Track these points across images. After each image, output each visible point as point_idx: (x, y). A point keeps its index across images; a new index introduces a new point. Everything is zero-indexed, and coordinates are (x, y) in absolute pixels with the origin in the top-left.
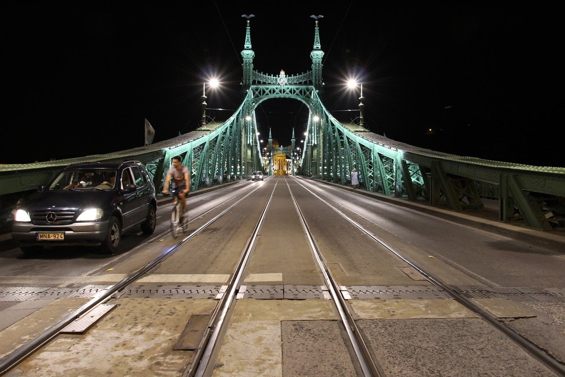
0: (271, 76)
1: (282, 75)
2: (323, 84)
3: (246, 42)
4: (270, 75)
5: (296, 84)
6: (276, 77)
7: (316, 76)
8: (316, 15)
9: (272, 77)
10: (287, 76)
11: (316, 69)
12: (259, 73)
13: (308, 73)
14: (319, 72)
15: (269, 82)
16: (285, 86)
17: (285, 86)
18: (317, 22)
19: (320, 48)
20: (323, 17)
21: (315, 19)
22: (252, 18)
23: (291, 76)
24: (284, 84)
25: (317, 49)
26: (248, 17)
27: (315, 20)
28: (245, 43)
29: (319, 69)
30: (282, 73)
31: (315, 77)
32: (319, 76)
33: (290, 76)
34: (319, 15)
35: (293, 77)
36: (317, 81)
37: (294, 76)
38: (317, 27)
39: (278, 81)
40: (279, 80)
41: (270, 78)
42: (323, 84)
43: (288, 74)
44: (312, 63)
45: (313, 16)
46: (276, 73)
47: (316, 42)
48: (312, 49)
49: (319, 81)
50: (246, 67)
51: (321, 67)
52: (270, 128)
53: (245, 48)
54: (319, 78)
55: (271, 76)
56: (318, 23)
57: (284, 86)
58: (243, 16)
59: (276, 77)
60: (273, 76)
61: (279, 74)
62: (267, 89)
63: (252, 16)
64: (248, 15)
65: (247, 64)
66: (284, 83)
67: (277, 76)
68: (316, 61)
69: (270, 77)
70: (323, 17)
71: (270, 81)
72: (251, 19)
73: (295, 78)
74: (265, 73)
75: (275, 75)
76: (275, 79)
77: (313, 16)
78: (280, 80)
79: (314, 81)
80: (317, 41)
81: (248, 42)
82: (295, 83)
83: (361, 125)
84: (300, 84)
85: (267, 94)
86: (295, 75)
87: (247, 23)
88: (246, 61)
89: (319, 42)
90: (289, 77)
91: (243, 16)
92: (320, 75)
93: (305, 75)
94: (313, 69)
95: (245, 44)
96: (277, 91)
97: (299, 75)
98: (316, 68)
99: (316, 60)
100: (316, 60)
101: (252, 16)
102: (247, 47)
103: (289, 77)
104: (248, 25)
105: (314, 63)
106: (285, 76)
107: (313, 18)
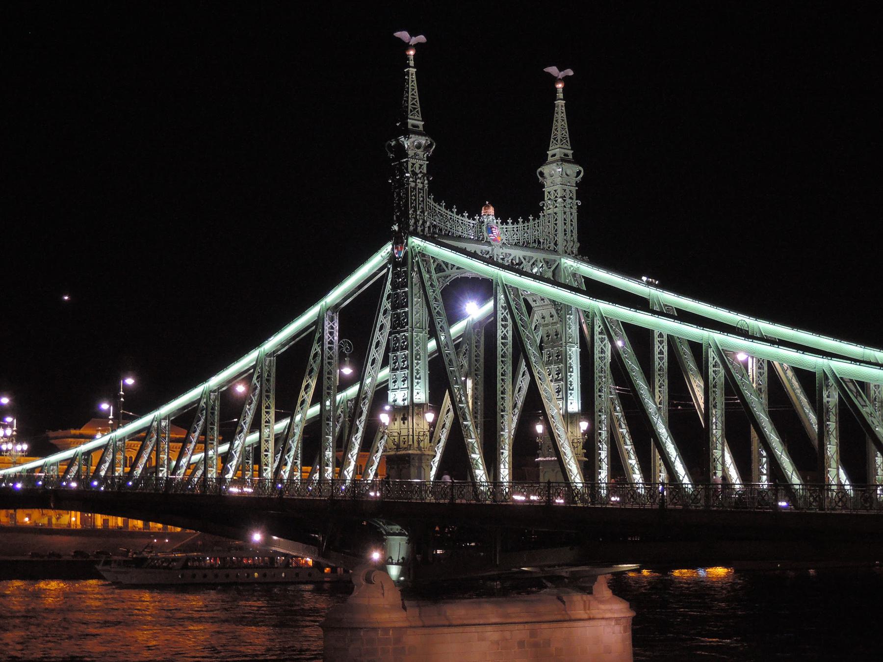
0: (463, 216)
3: (411, 111)
4: (460, 212)
7: (565, 231)
8: (561, 70)
10: (499, 221)
18: (560, 86)
25: (564, 160)
27: (554, 80)
29: (571, 214)
38: (561, 99)
39: (485, 234)
41: (460, 221)
45: (553, 70)
46: (474, 211)
50: (413, 181)
53: (410, 127)
58: (398, 34)
60: (469, 217)
63: (422, 38)
64: (413, 34)
69: (459, 217)
74: (449, 207)
77: (553, 70)
87: (407, 58)
88: (413, 164)
90: (502, 223)
91: (398, 34)
95: (410, 116)
98: (567, 210)
101: (422, 38)
102: (414, 126)
104: (412, 63)
107: (549, 74)
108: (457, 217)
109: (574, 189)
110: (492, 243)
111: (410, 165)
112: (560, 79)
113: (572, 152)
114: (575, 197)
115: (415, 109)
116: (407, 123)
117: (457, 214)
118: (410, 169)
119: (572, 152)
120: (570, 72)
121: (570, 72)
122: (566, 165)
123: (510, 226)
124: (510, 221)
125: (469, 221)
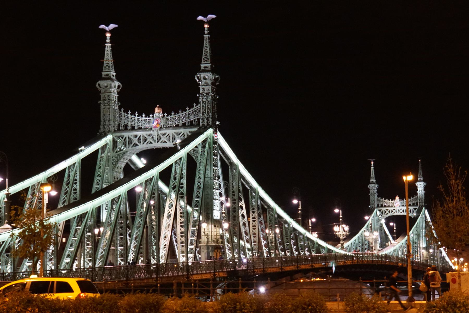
0: (142, 116)
2: (218, 123)
3: (105, 67)
5: (177, 126)
6: (149, 117)
8: (205, 16)
9: (144, 118)
10: (166, 115)
11: (203, 102)
12: (125, 113)
13: (195, 108)
14: (208, 106)
15: (140, 126)
16: (158, 131)
17: (158, 131)
18: (206, 26)
19: (210, 68)
20: (214, 16)
21: (204, 21)
22: (114, 29)
23: (171, 115)
24: (158, 128)
26: (107, 29)
27: (202, 22)
28: (102, 69)
30: (157, 110)
31: (203, 114)
32: (208, 112)
33: (169, 114)
34: (208, 15)
35: (173, 116)
36: (205, 120)
37: (175, 114)
38: (206, 34)
39: (151, 124)
40: (152, 122)
42: (218, 123)
43: (167, 111)
44: (199, 93)
45: (200, 18)
46: (149, 112)
47: (204, 59)
48: (199, 70)
51: (210, 97)
52: (371, 162)
55: (142, 116)
56: (209, 29)
57: (157, 131)
59: (149, 117)
61: (153, 113)
62: (136, 136)
63: (112, 26)
64: (107, 25)
65: (105, 102)
66: (159, 126)
67: (151, 116)
68: (203, 89)
70: (214, 16)
71: (140, 124)
72: (111, 31)
73: (177, 118)
74: (133, 113)
75: (147, 115)
76: (148, 120)
77: (200, 18)
78: (153, 123)
79: (201, 121)
80: (206, 57)
81: (107, 67)
82: (177, 124)
83: (6, 222)
84: (184, 126)
85: (137, 145)
86: (177, 112)
87: (105, 37)
89: (208, 59)
92: (210, 110)
93: (191, 112)
94: (200, 100)
95: (104, 71)
96: (149, 139)
97: (182, 112)
98: (204, 100)
99: (203, 87)
100: (203, 87)
101: (112, 26)
103: (168, 116)
105: (201, 92)
106: (161, 115)
108: (138, 118)
109: (210, 88)
110: (153, 129)
112: (206, 22)
113: (210, 64)
114: (210, 91)
115: (107, 66)
116: (102, 74)
117: (138, 116)
118: (102, 99)
119: (210, 64)
120: (211, 16)
121: (211, 16)
122: (202, 75)
124: (173, 113)
125: (146, 118)
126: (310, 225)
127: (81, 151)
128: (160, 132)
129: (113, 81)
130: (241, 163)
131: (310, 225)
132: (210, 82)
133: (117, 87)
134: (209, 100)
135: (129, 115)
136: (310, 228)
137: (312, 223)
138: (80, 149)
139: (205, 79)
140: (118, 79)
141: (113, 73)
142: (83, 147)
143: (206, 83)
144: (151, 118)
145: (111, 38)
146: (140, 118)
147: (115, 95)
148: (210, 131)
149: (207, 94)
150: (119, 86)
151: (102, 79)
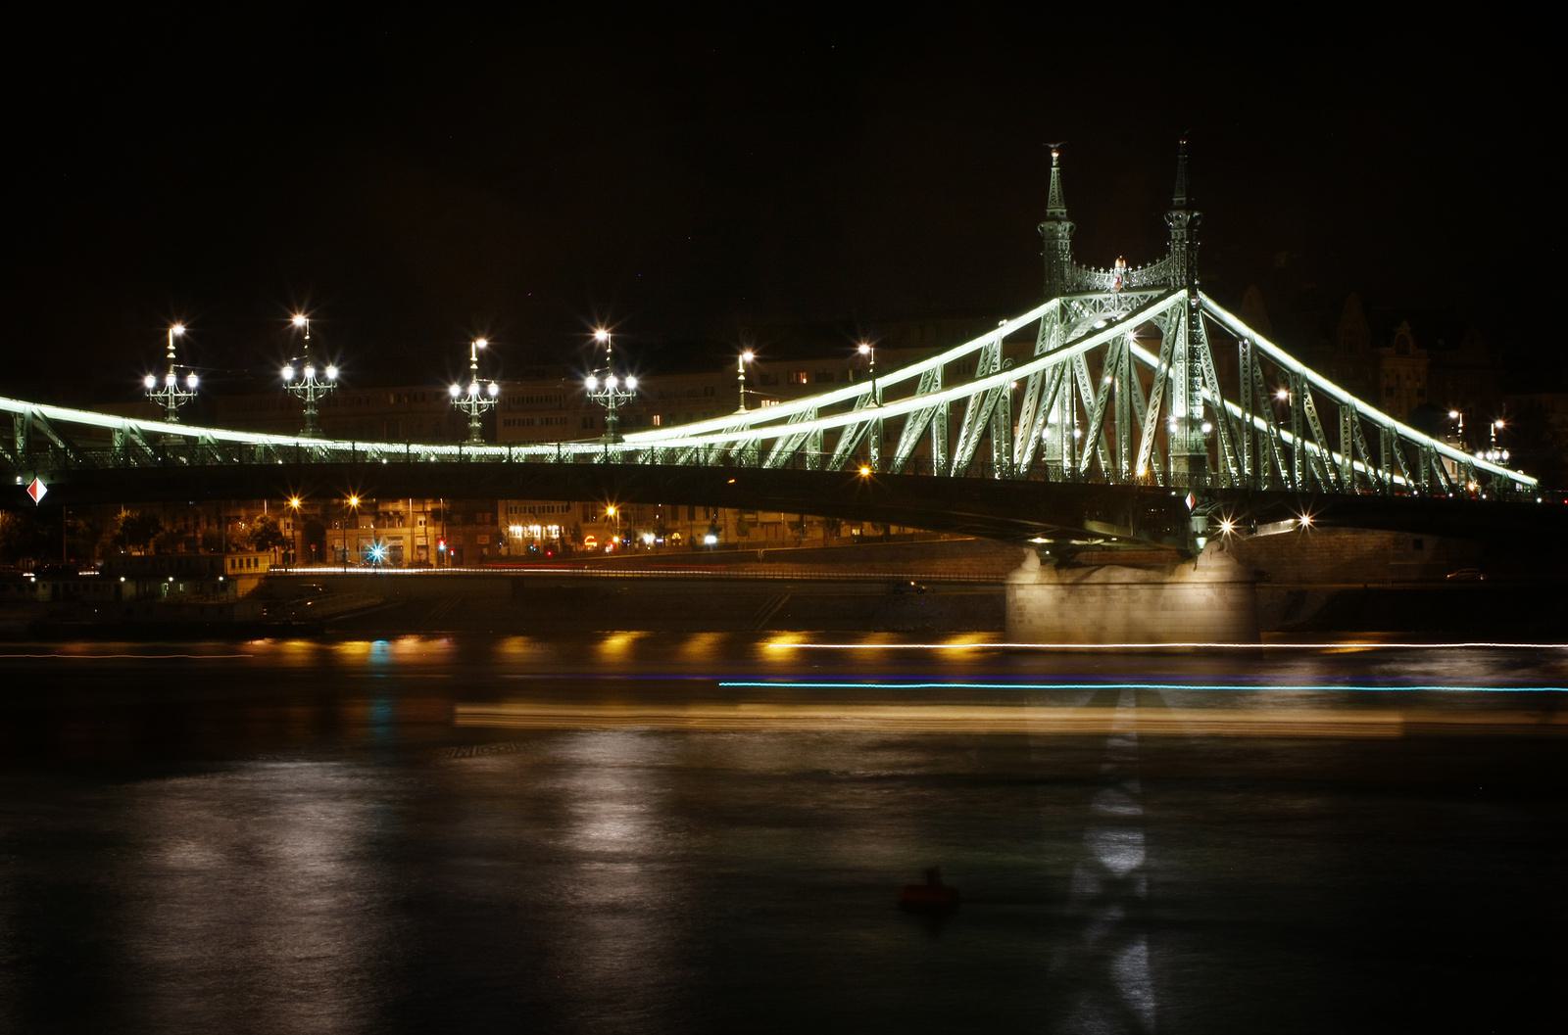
1: (1118, 270)
4: (1097, 270)
6: (1109, 272)
29: (1182, 252)
30: (1118, 263)
43: (1132, 263)
44: (1169, 239)
46: (1109, 266)
49: (1180, 277)
53: (1048, 215)
54: (1182, 270)
59: (1109, 272)
61: (1114, 267)
67: (1111, 271)
75: (1107, 270)
105: (1173, 237)
109: (1184, 231)
111: (1046, 245)
123: (1102, 274)
126: (1493, 434)
127: (1002, 325)
128: (1122, 295)
129: (1059, 221)
130: (1268, 339)
131: (1493, 434)
132: (1184, 224)
133: (1068, 230)
134: (1183, 249)
135: (1084, 271)
136: (1493, 440)
137: (1496, 429)
138: (1000, 323)
139: (1178, 218)
140: (1070, 218)
141: (1061, 210)
142: (1005, 321)
143: (1180, 225)
144: (1111, 274)
145: (1058, 159)
146: (1097, 274)
147: (1065, 243)
148: (1183, 293)
149: (1181, 240)
150: (1071, 228)
151: (1046, 219)
